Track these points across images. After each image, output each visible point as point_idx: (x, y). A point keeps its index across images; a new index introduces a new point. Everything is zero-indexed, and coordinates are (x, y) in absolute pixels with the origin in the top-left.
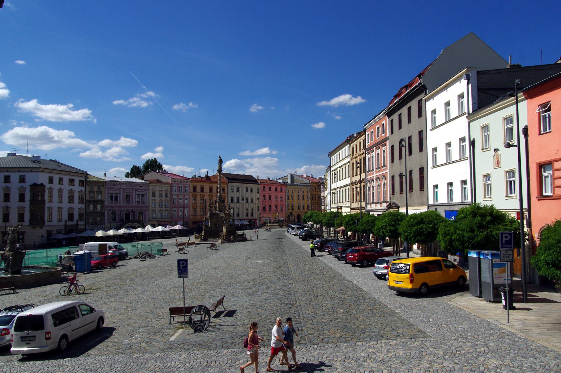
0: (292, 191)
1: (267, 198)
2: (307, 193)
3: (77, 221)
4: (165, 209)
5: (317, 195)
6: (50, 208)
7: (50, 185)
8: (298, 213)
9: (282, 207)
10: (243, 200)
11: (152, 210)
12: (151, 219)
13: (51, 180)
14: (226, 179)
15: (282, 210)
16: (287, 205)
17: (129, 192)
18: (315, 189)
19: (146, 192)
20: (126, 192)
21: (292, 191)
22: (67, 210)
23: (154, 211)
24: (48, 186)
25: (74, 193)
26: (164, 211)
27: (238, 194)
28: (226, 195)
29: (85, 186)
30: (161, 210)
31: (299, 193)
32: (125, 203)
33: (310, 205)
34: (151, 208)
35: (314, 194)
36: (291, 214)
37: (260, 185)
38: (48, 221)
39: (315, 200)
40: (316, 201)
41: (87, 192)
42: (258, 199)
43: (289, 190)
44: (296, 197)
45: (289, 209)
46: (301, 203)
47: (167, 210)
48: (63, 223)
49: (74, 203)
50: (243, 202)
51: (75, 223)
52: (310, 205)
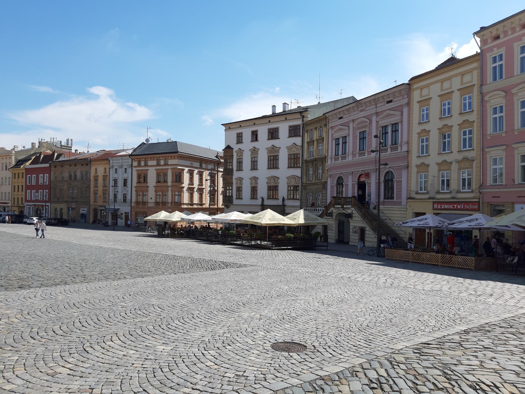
3: (284, 199)
4: (460, 157)
6: (240, 179)
7: (240, 146)
11: (417, 166)
12: (414, 195)
13: (239, 138)
17: (364, 127)
19: (398, 113)
20: (358, 128)
22: (267, 181)
23: (424, 167)
24: (236, 147)
25: (278, 151)
26: (454, 166)
29: (301, 134)
30: (445, 161)
32: (357, 155)
34: (415, 161)
38: (237, 199)
41: (306, 145)
47: (465, 159)
48: (259, 202)
49: (257, 169)
51: (280, 202)
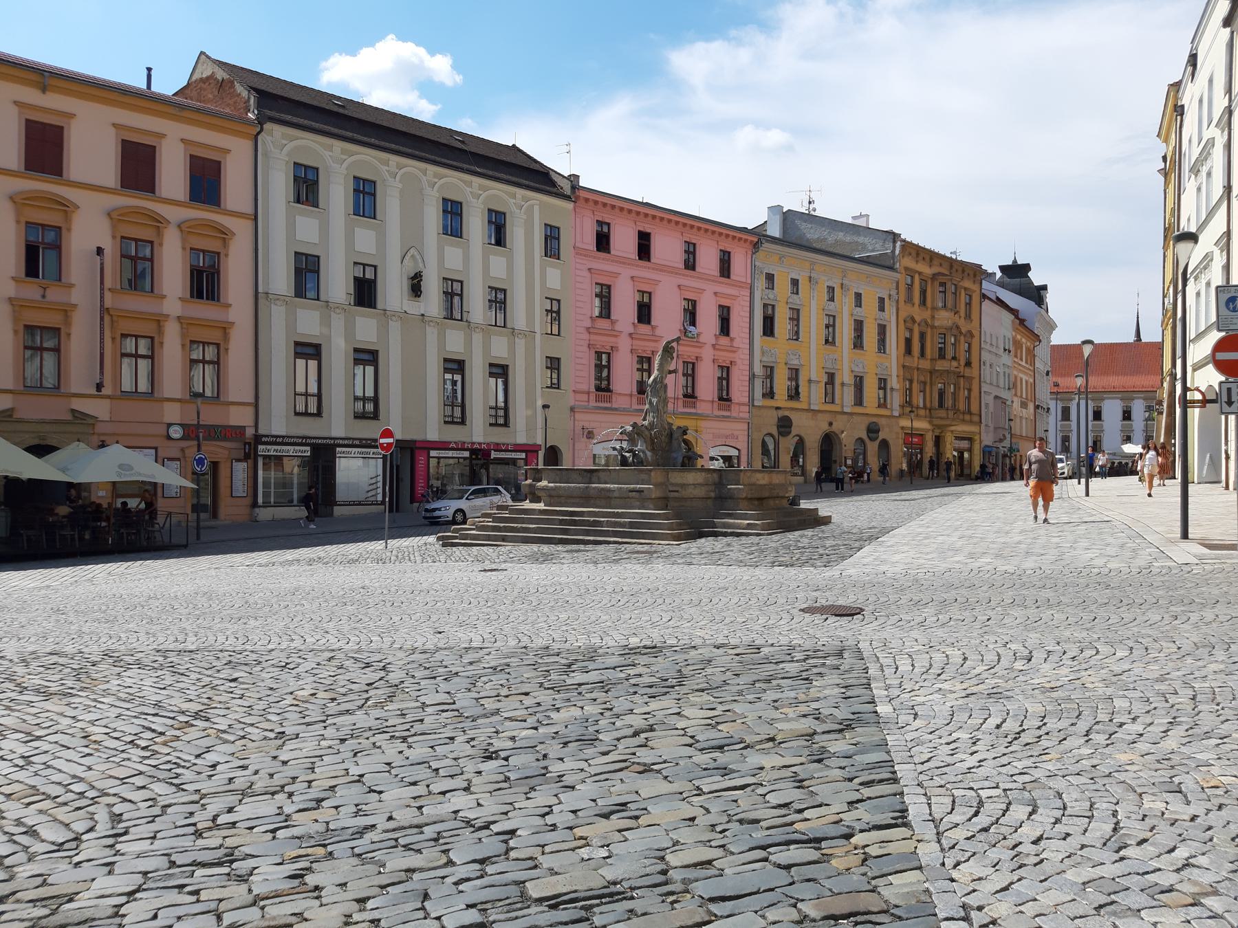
0: (795, 283)
1: (624, 308)
2: (882, 309)
5: (933, 327)
8: (825, 427)
9: (725, 379)
10: (416, 288)
14: (245, 94)
15: (724, 398)
16: (758, 370)
18: (923, 293)
21: (795, 283)
27: (365, 240)
28: (241, 229)
31: (832, 299)
33: (894, 382)
35: (918, 319)
36: (785, 425)
37: (569, 206)
39: (923, 354)
40: (925, 364)
42: (555, 314)
43: (770, 278)
44: (813, 326)
45: (770, 394)
46: (846, 362)
50: (414, 307)
52: (894, 382)
